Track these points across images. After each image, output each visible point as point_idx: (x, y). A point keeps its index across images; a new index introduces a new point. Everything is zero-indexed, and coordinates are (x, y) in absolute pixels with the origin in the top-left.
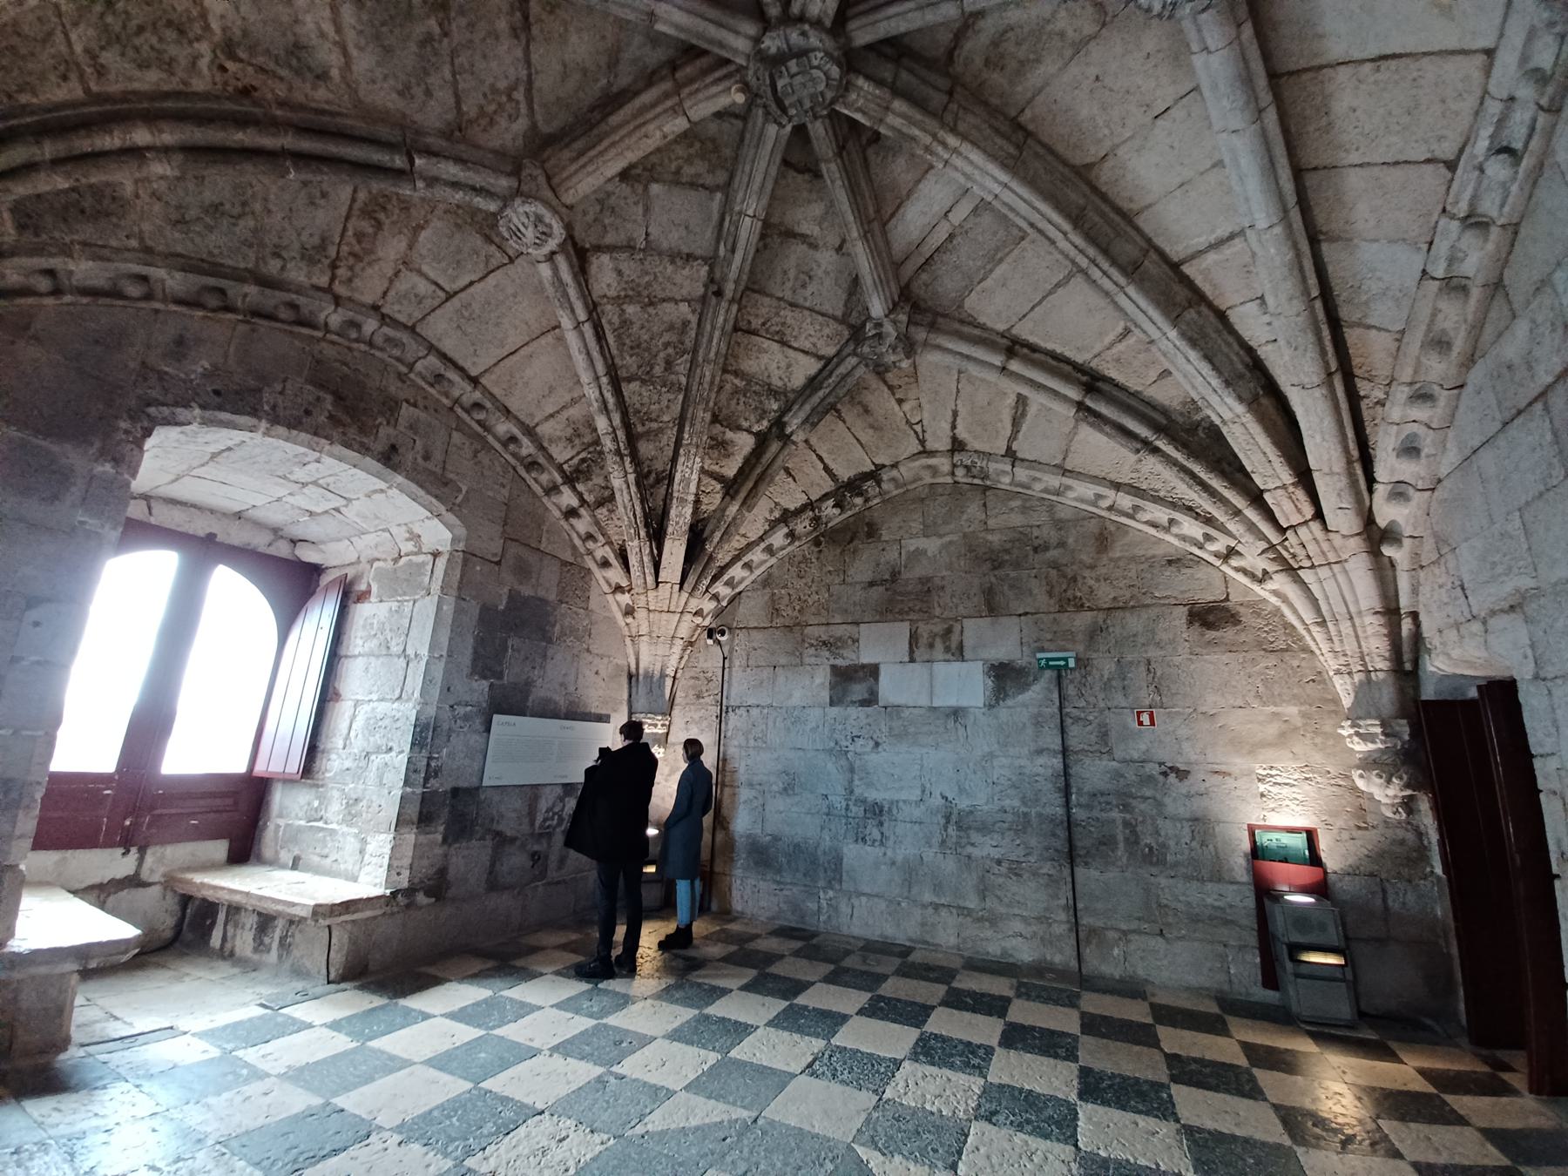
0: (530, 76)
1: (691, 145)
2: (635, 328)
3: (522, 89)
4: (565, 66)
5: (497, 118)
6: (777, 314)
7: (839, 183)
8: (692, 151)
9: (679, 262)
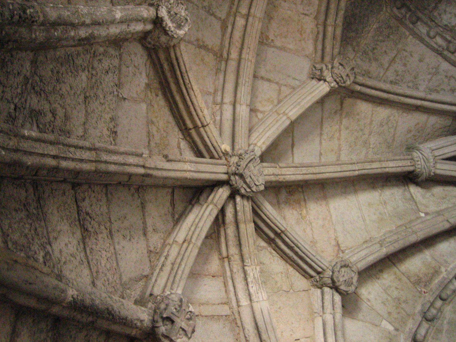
1: (164, 131)
6: (99, 225)
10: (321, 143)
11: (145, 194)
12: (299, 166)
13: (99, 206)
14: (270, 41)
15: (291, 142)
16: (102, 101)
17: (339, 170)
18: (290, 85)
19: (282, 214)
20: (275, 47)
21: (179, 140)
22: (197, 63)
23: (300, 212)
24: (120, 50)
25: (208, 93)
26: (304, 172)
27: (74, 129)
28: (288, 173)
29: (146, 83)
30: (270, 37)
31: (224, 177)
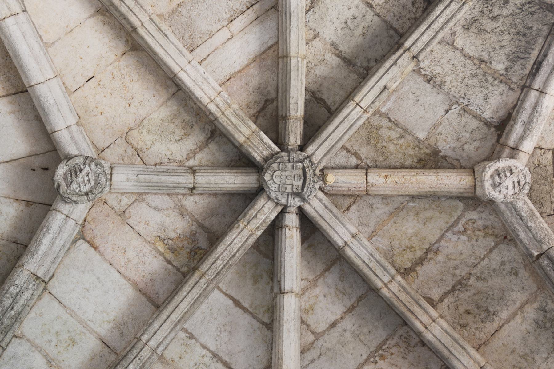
0: (447, 231)
1: (383, 147)
2: (508, 50)
3: (456, 229)
4: (425, 223)
5: (482, 229)
7: (292, 101)
8: (385, 144)
9: (438, 80)
10: (204, 347)
11: (356, 77)
12: (230, 262)
13: (396, 13)
14: (377, 359)
15: (243, 304)
16: (466, 81)
17: (173, 317)
18: (309, 349)
19: (188, 217)
20: (366, 361)
21: (361, 159)
22: (413, 238)
23: (166, 242)
24: (495, 127)
25: (374, 233)
26: (219, 261)
27: (466, 35)
28: (238, 238)
29: (440, 151)
30: (382, 362)
31: (310, 150)
